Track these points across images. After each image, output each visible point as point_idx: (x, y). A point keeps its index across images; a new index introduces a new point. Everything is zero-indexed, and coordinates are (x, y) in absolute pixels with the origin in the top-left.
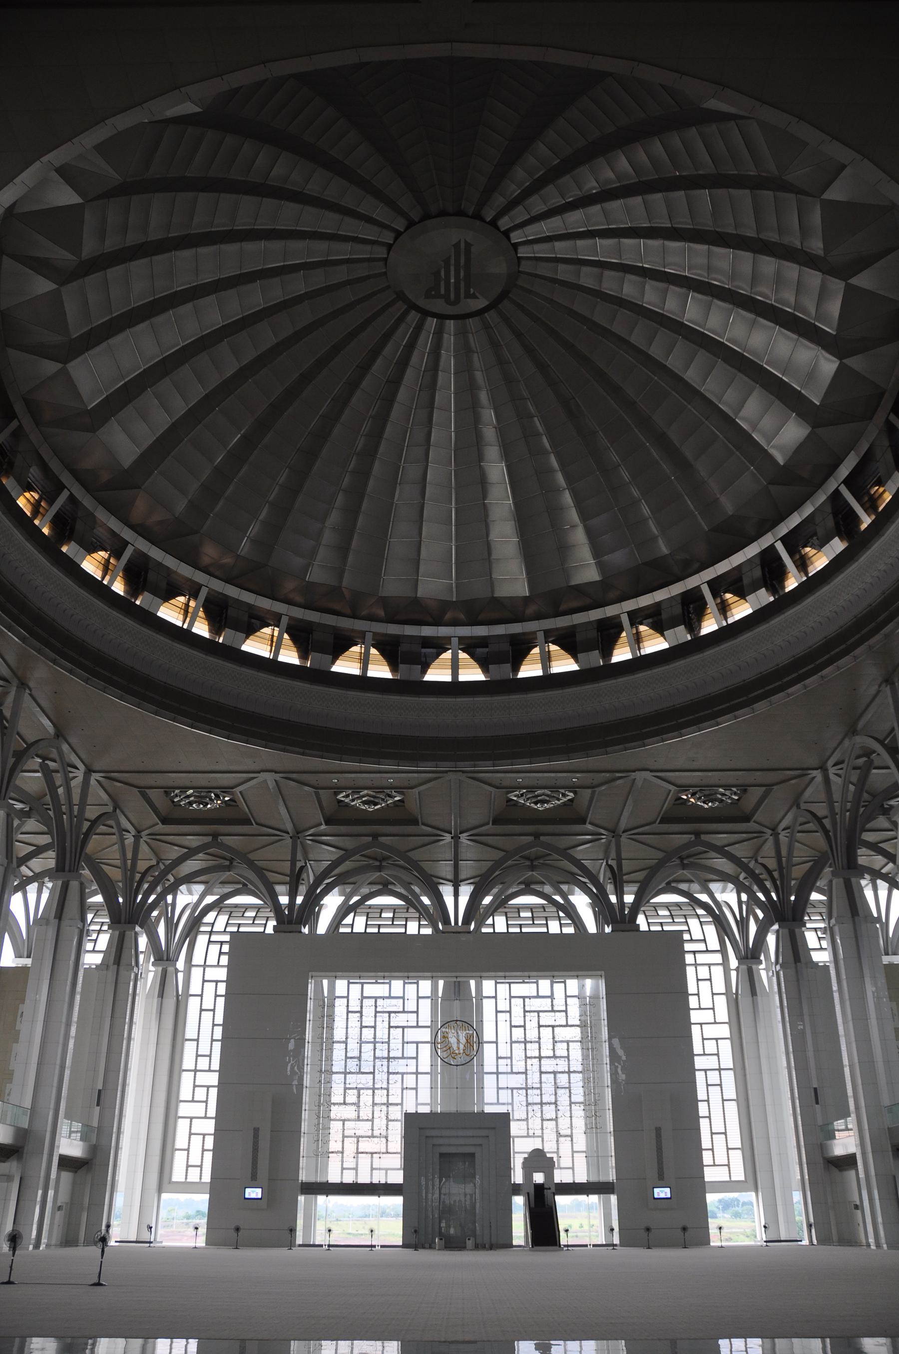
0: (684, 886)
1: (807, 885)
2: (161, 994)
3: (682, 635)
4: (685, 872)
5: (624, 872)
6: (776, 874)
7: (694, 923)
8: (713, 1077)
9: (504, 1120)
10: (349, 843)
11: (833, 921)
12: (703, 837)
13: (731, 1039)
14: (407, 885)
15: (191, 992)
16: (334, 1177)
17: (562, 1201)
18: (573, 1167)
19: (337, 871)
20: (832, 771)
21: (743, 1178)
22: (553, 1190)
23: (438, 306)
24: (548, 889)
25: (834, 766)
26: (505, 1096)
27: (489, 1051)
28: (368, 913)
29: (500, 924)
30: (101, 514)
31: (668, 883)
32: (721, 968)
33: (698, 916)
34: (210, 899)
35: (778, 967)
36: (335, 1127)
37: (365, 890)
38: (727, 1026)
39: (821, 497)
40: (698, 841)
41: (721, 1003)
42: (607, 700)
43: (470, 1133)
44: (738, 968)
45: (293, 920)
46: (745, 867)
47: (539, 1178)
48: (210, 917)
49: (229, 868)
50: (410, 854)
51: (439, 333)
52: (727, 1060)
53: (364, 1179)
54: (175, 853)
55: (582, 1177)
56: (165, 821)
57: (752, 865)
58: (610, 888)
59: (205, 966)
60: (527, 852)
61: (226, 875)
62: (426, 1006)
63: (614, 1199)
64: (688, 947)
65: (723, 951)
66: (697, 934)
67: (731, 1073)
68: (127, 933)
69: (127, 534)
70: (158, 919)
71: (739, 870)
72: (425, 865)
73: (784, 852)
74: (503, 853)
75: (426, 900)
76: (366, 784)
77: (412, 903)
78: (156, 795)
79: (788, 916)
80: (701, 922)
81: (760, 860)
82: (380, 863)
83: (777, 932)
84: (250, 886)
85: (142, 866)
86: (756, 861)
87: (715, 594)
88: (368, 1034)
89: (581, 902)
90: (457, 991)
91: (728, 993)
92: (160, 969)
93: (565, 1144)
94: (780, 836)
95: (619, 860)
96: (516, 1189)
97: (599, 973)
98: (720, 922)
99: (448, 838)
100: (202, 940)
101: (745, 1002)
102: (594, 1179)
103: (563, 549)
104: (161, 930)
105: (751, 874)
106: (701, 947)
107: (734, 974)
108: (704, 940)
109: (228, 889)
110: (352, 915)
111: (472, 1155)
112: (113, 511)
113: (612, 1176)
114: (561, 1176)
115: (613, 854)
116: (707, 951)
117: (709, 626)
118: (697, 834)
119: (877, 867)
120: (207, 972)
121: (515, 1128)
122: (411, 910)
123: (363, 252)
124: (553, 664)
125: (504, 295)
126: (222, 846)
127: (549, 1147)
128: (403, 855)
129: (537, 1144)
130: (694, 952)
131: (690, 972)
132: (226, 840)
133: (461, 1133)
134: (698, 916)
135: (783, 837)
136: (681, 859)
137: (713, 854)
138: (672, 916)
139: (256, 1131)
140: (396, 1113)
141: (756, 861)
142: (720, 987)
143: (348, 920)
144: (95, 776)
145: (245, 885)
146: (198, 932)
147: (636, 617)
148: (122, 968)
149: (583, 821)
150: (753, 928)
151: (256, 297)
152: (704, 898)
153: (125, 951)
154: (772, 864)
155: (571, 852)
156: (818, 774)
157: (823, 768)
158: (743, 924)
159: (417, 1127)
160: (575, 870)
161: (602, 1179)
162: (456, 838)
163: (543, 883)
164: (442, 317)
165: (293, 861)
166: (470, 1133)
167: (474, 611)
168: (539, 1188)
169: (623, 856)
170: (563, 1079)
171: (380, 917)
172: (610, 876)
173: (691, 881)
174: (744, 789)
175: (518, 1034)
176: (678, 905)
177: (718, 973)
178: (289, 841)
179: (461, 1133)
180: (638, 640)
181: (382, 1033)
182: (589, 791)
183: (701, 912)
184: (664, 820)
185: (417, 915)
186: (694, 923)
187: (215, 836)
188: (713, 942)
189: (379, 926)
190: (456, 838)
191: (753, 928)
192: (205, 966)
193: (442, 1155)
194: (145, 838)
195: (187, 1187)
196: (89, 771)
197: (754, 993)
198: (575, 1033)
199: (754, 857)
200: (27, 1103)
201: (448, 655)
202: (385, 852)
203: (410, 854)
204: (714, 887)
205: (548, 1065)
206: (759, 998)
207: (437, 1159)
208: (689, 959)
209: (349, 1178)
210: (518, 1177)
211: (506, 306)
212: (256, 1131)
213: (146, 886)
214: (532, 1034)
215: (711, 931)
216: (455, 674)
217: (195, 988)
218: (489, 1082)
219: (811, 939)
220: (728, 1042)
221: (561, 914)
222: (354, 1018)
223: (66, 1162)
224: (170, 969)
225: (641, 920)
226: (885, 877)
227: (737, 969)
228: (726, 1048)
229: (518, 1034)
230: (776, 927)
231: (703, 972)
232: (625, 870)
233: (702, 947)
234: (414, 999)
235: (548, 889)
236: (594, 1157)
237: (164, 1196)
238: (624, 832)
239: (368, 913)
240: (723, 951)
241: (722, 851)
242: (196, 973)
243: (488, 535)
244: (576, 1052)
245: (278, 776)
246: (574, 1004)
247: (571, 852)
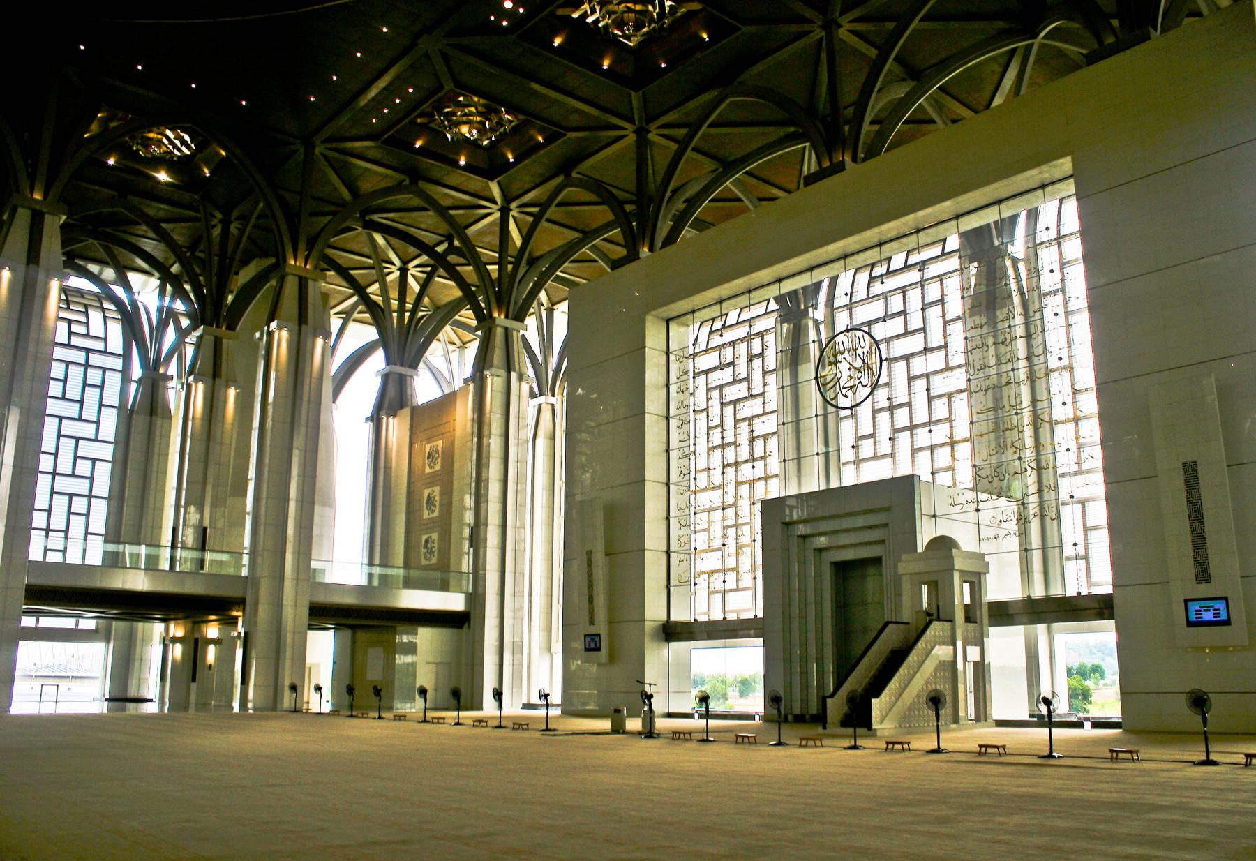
0: (94, 268)
7: (95, 317)
8: (79, 505)
13: (113, 462)
25: (324, 142)
32: (119, 375)
33: (103, 310)
38: (111, 447)
52: (102, 485)
65: (126, 357)
67: (105, 502)
80: (105, 318)
83: (200, 338)
91: (121, 407)
94: (233, 226)
98: (130, 318)
101: (140, 422)
106: (99, 346)
107: (133, 386)
108: (105, 339)
116: (105, 352)
134: (103, 310)
135: (233, 228)
142: (112, 397)
152: (119, 291)
176: (81, 293)
177: (114, 381)
183: (108, 305)
186: (95, 317)
188: (116, 344)
191: (170, 336)
204: (133, 277)
220: (109, 465)
227: (139, 382)
228: (104, 473)
231: (94, 377)
233: (99, 346)
240: (126, 357)
241: (155, 224)
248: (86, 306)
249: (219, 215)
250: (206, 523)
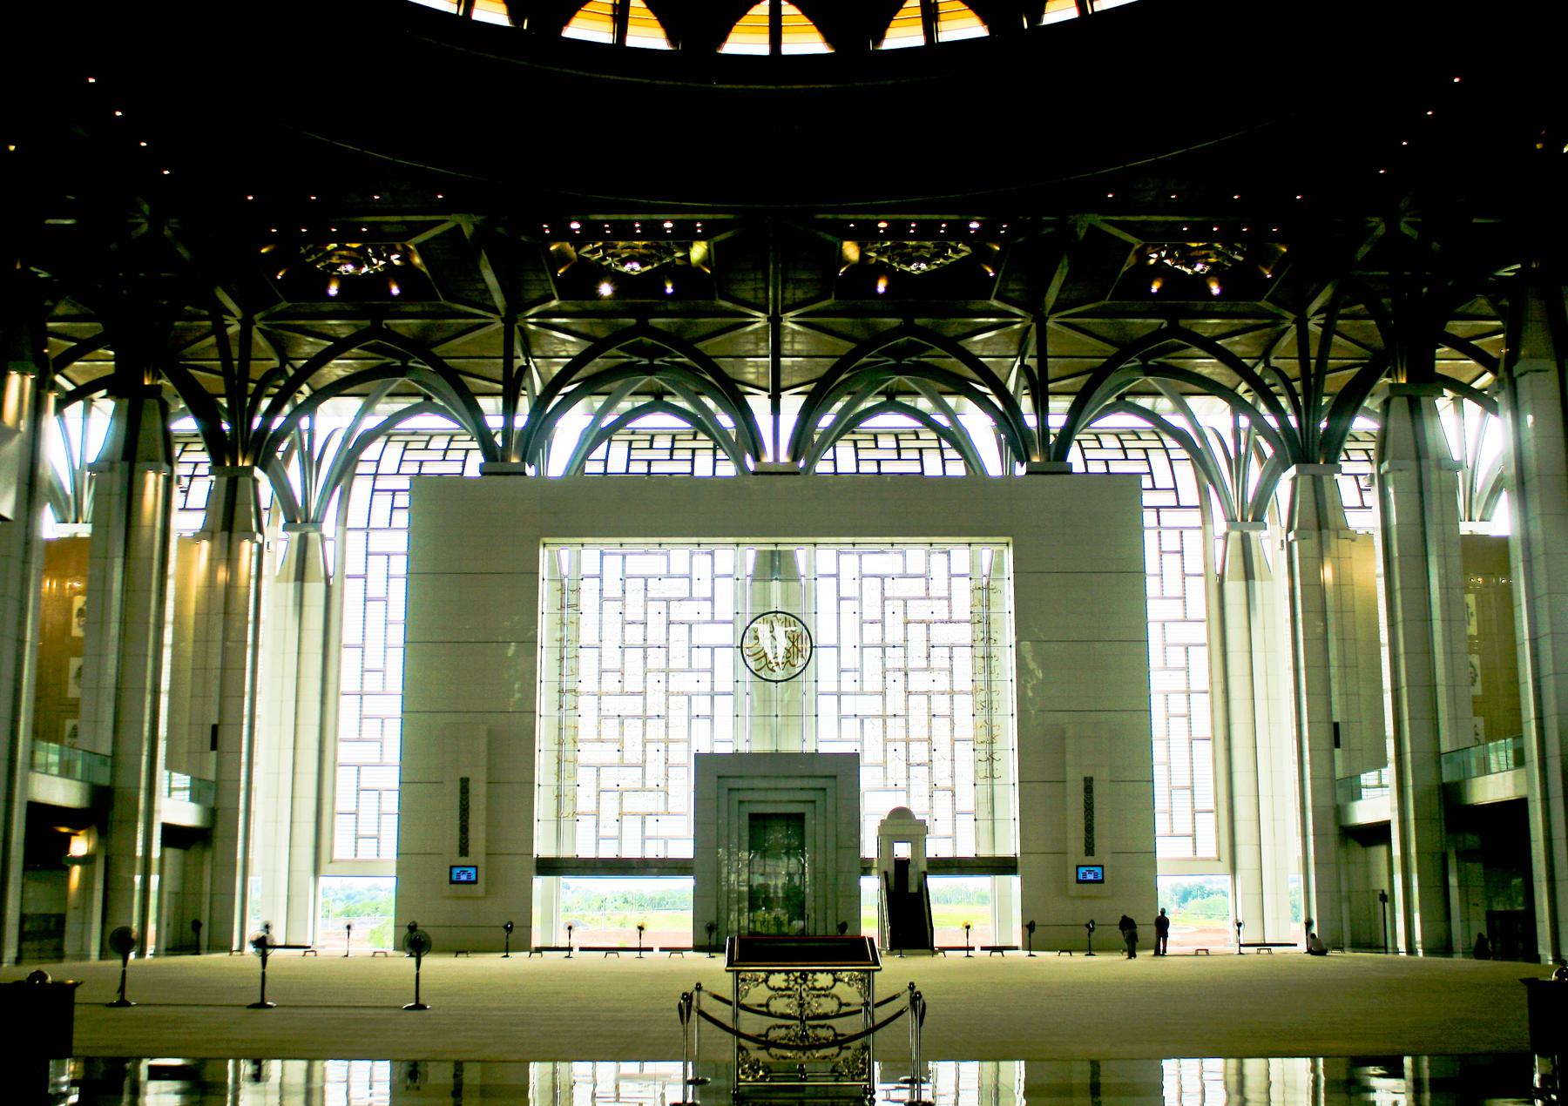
0: (1145, 402)
1: (1349, 402)
2: (301, 576)
4: (1150, 379)
5: (1050, 377)
6: (1297, 385)
7: (1158, 459)
9: (849, 764)
11: (1385, 466)
14: (693, 398)
15: (348, 571)
17: (937, 885)
19: (582, 373)
21: (1213, 854)
22: (924, 867)
24: (923, 404)
26: (851, 728)
27: (825, 659)
28: (631, 442)
29: (844, 458)
31: (1121, 397)
33: (1166, 450)
34: (370, 422)
35: (1291, 536)
37: (626, 405)
41: (1197, 588)
43: (798, 783)
44: (1227, 534)
46: (1246, 374)
47: (903, 850)
48: (372, 452)
50: (700, 346)
53: (631, 851)
54: (309, 347)
55: (966, 850)
57: (1258, 370)
58: (1026, 404)
59: (368, 529)
60: (896, 345)
62: (725, 589)
63: (1014, 882)
64: (1149, 499)
66: (1164, 479)
68: (241, 480)
70: (288, 455)
71: (1238, 378)
72: (726, 365)
73: (1314, 351)
74: (852, 346)
75: (725, 421)
77: (701, 424)
79: (1312, 451)
80: (1170, 461)
81: (1274, 363)
83: (1294, 479)
84: (436, 400)
85: (257, 370)
86: (1267, 364)
88: (634, 634)
89: (978, 425)
90: (775, 566)
92: (296, 535)
93: (943, 799)
95: (1042, 357)
97: (1004, 539)
98: (1200, 460)
99: (761, 320)
100: (361, 487)
101: (1235, 589)
102: (985, 852)
104: (294, 472)
105: (1257, 385)
106: (1169, 499)
109: (401, 404)
110: (605, 444)
111: (800, 818)
114: (937, 847)
115: (1032, 349)
119: (1465, 380)
120: (372, 545)
121: (868, 778)
122: (701, 436)
124: (942, 26)
126: (391, 335)
129: (900, 801)
130: (1158, 509)
131: (1150, 538)
133: (783, 783)
134: (1166, 450)
136: (1144, 358)
137: (1196, 351)
138: (1124, 449)
139: (465, 785)
141: (1267, 364)
142: (1195, 563)
143: (600, 452)
145: (428, 398)
146: (354, 475)
148: (235, 536)
150: (1255, 472)
152: (1179, 421)
153: (239, 510)
154: (1292, 367)
155: (962, 343)
158: (1238, 464)
160: (969, 373)
162: (775, 322)
163: (916, 394)
165: (509, 357)
166: (798, 783)
168: (902, 865)
169: (1050, 350)
170: (941, 704)
171: (651, 447)
172: (1024, 382)
173: (1157, 394)
175: (872, 634)
176: (1134, 432)
177: (1193, 540)
178: (499, 325)
179: (783, 783)
181: (656, 633)
183: (1170, 442)
185: (710, 444)
186: (1158, 459)
188: (1190, 495)
189: (649, 462)
190: (775, 322)
191: (1255, 472)
192: (368, 529)
193: (754, 817)
194: (260, 325)
195: (358, 868)
197: (1248, 574)
199: (1265, 357)
200: (105, 748)
202: (659, 346)
203: (700, 346)
204: (1193, 402)
206: (1257, 583)
207: (745, 821)
208: (1149, 518)
209: (608, 851)
210: (869, 849)
212: (465, 785)
213: (265, 403)
214: (894, 634)
215: (1186, 472)
217: (354, 564)
218: (827, 706)
219: (1348, 491)
221: (945, 444)
222: (612, 609)
223: (173, 835)
224: (313, 536)
225: (1074, 457)
226: (1476, 395)
229: (872, 634)
230: (1293, 471)
232: (1051, 374)
233: (1169, 499)
234: (708, 575)
235: (923, 404)
237: (321, 879)
238: (1053, 311)
239: (631, 442)
240: (1204, 507)
241: (1210, 346)
242: (355, 541)
246: (962, 589)
247: (962, 343)
248: (1145, 450)
249: (1291, 316)
250: (1336, 719)
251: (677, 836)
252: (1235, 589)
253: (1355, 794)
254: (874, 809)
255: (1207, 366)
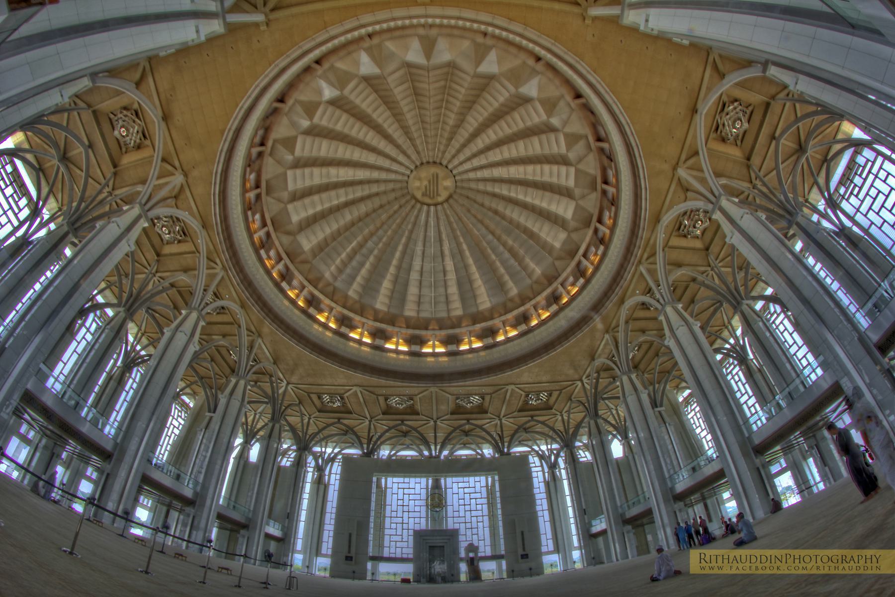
3: (523, 327)
10: (392, 423)
12: (535, 418)
14: (418, 446)
16: (386, 554)
18: (485, 549)
20: (585, 381)
23: (427, 200)
30: (296, 273)
36: (387, 538)
39: (573, 264)
40: (533, 420)
42: (496, 355)
45: (369, 454)
47: (471, 555)
49: (345, 435)
51: (428, 212)
53: (399, 555)
56: (319, 411)
60: (466, 422)
61: (344, 438)
65: (542, 466)
69: (306, 283)
76: (398, 395)
78: (314, 397)
82: (405, 434)
87: (536, 310)
95: (502, 431)
96: (462, 559)
99: (432, 423)
100: (336, 464)
101: (552, 485)
103: (475, 297)
105: (554, 431)
112: (301, 273)
113: (503, 553)
114: (480, 555)
117: (534, 322)
118: (532, 417)
121: (461, 538)
123: (400, 177)
125: (450, 196)
127: (476, 544)
128: (415, 429)
132: (345, 422)
139: (350, 535)
140: (411, 532)
144: (290, 386)
147: (504, 323)
149: (486, 412)
150: (553, 458)
151: (359, 192)
156: (579, 383)
157: (581, 380)
158: (550, 456)
159: (420, 536)
161: (498, 553)
162: (435, 422)
164: (429, 205)
167: (442, 324)
174: (550, 395)
177: (540, 474)
180: (506, 332)
182: (489, 396)
184: (520, 411)
187: (339, 419)
190: (435, 422)
191: (553, 458)
196: (288, 383)
198: (485, 501)
201: (431, 343)
205: (474, 513)
210: (463, 554)
211: (451, 201)
212: (350, 535)
216: (434, 349)
229: (461, 502)
236: (494, 544)
240: (542, 466)
241: (543, 423)
243: (446, 291)
244: (485, 507)
245: (361, 389)
251: (409, 552)
252: (552, 485)
253: (591, 526)
254: (463, 545)
255: (539, 428)
